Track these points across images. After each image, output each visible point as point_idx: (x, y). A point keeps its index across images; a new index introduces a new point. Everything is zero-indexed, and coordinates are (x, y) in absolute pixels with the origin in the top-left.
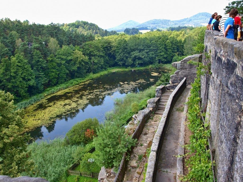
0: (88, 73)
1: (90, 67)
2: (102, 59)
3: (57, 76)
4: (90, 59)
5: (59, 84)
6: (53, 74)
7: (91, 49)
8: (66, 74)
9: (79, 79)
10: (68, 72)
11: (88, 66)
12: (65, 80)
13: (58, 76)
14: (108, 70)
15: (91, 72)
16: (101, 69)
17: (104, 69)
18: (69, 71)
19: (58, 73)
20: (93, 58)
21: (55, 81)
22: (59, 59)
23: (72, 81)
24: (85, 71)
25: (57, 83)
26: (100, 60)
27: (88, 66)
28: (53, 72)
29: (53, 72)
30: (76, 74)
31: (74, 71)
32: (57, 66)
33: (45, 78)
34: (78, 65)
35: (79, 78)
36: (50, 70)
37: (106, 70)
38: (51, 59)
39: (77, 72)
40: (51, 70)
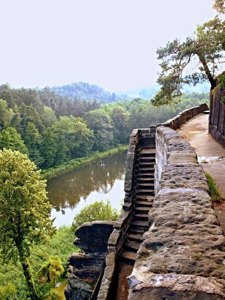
0: (93, 151)
1: (95, 143)
2: (111, 133)
3: (55, 155)
4: (95, 133)
5: (56, 165)
6: (51, 152)
7: (97, 121)
8: (65, 152)
9: (81, 159)
10: (68, 149)
11: (94, 143)
12: (65, 160)
13: (56, 155)
14: (119, 147)
15: (97, 150)
16: (110, 145)
17: (113, 146)
18: (70, 148)
19: (56, 151)
20: (99, 131)
21: (52, 161)
22: (58, 134)
23: (73, 161)
24: (89, 149)
25: (54, 163)
26: (109, 135)
27: (94, 143)
28: (50, 150)
29: (50, 150)
30: (78, 152)
31: (75, 148)
32: (55, 143)
33: (40, 157)
34: (81, 142)
35: (82, 157)
36: (46, 148)
37: (116, 148)
38: (47, 133)
39: (80, 151)
40: (48, 148)
